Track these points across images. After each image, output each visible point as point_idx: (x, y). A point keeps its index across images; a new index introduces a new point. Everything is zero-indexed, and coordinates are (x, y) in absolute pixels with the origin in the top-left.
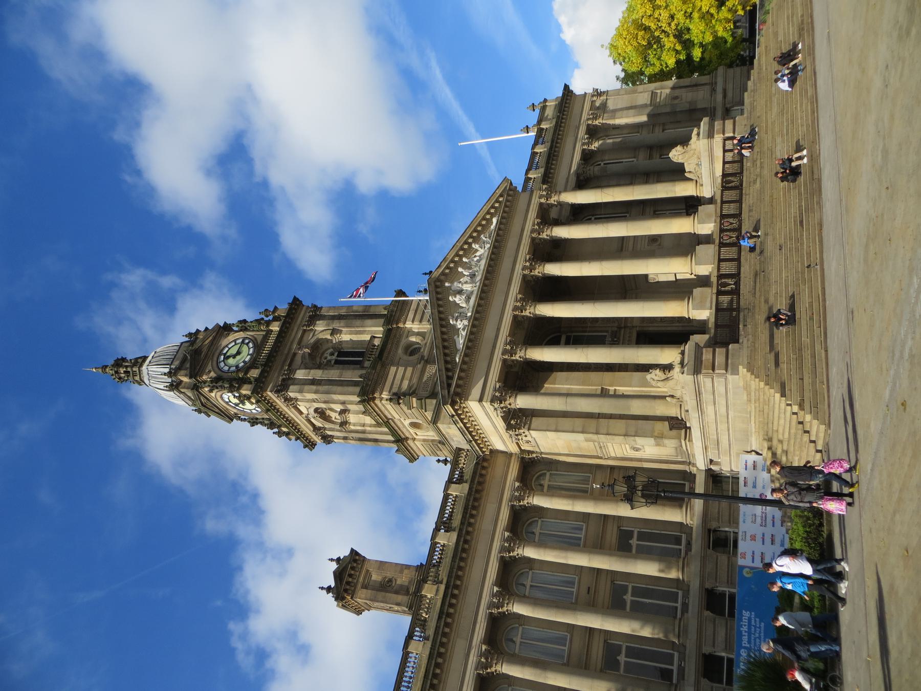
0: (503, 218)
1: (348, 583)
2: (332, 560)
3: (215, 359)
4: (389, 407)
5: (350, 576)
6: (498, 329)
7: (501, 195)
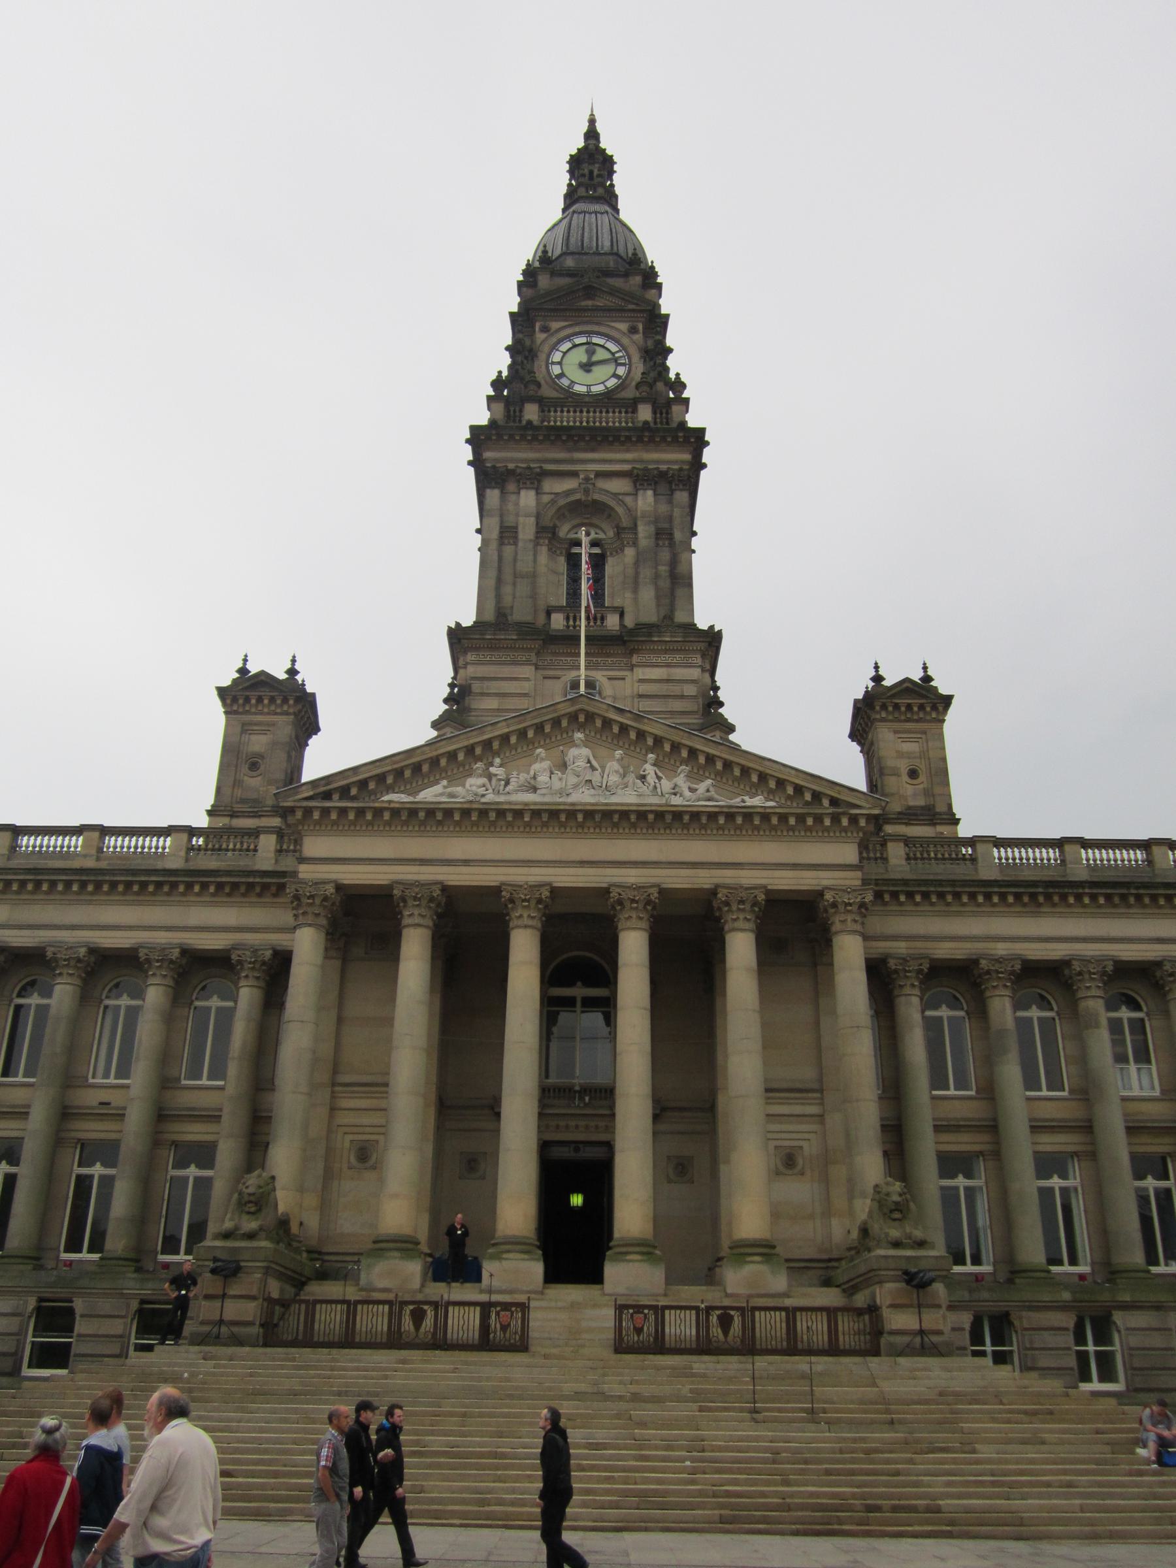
0: (765, 816)
1: (247, 700)
3: (577, 329)
5: (260, 700)
6: (466, 862)
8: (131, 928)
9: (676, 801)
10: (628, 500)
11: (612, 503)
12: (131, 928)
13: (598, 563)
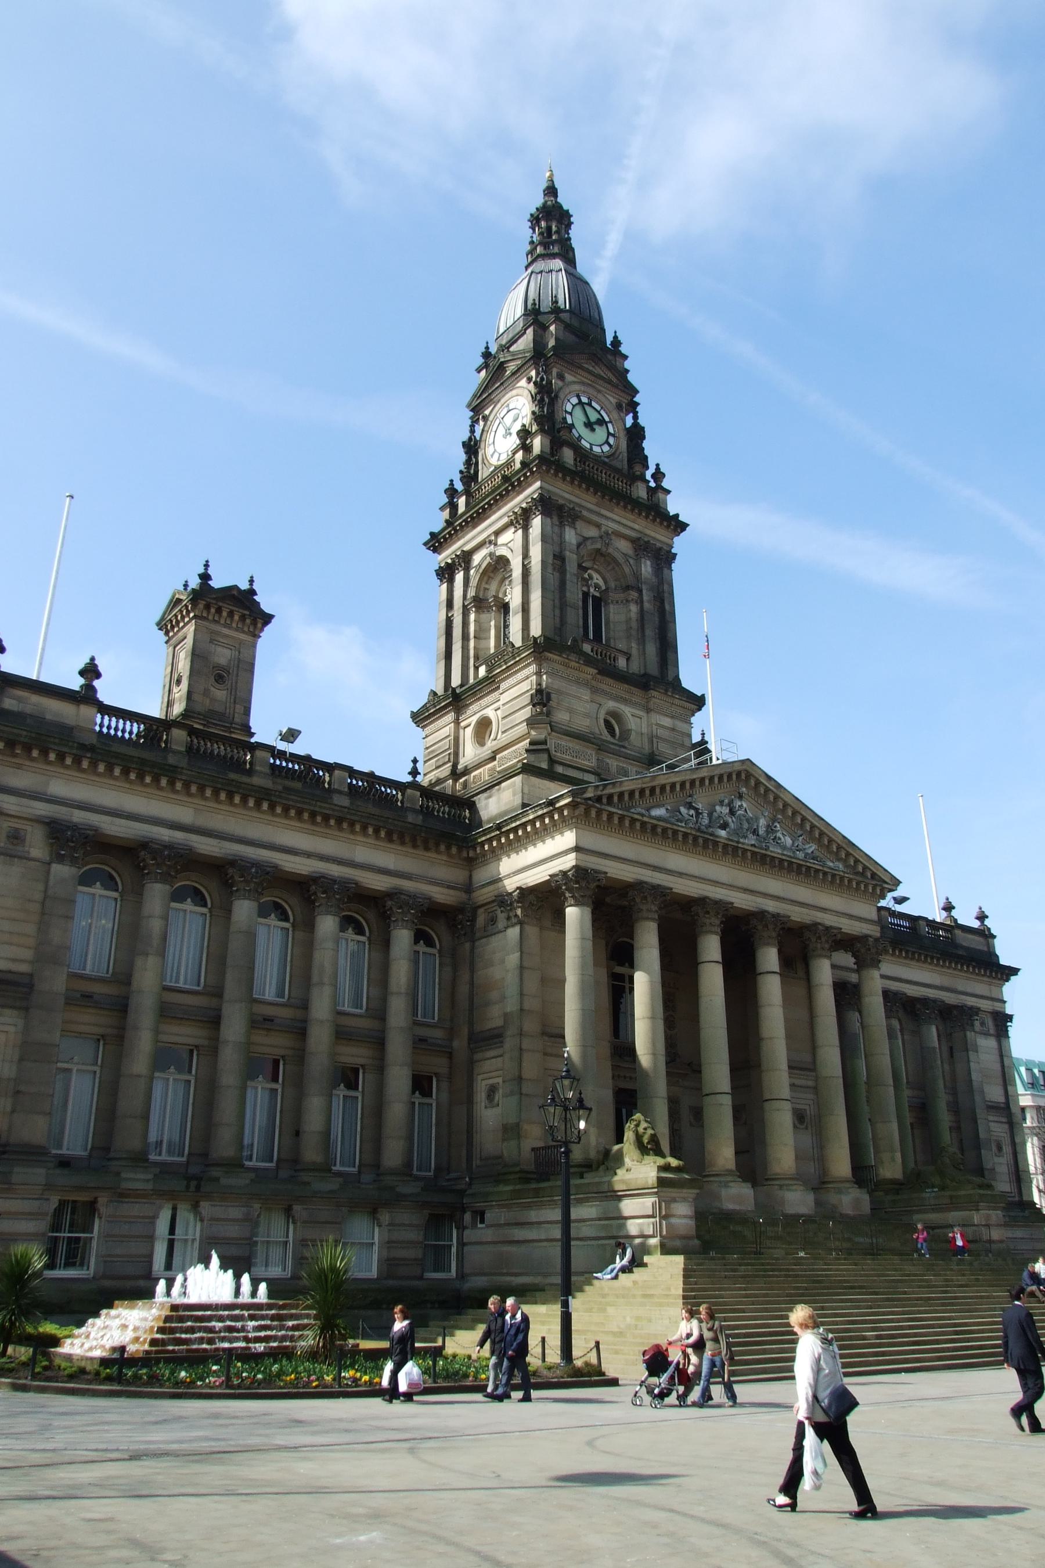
2: (251, 581)
4: (525, 686)
7: (874, 875)
8: (309, 855)
9: (800, 855)
10: (632, 561)
11: (621, 560)
12: (309, 855)
13: (598, 602)
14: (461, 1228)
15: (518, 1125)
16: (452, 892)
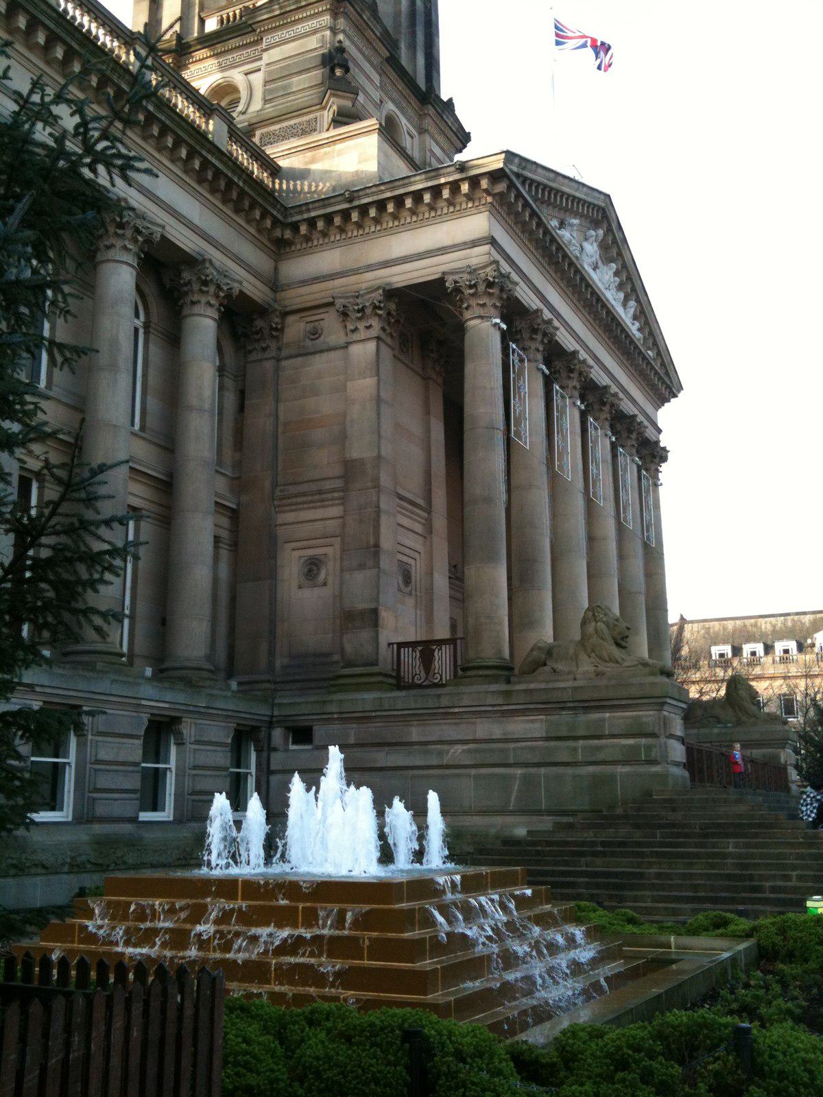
14: (265, 750)
15: (375, 612)
16: (258, 284)
